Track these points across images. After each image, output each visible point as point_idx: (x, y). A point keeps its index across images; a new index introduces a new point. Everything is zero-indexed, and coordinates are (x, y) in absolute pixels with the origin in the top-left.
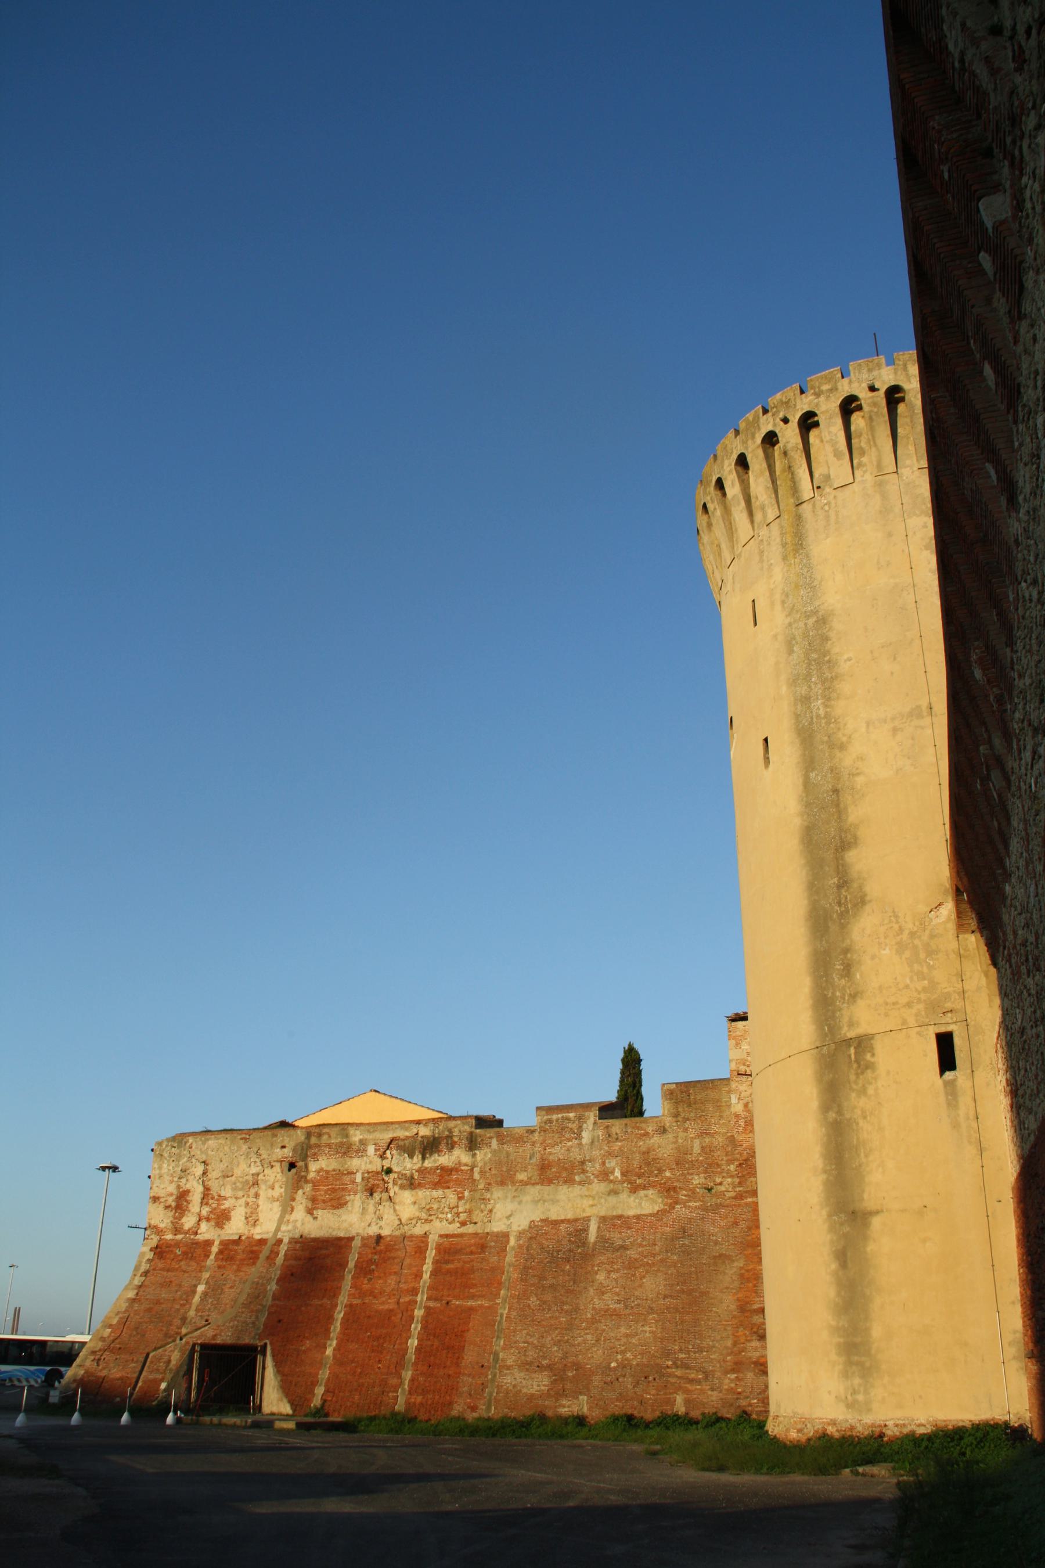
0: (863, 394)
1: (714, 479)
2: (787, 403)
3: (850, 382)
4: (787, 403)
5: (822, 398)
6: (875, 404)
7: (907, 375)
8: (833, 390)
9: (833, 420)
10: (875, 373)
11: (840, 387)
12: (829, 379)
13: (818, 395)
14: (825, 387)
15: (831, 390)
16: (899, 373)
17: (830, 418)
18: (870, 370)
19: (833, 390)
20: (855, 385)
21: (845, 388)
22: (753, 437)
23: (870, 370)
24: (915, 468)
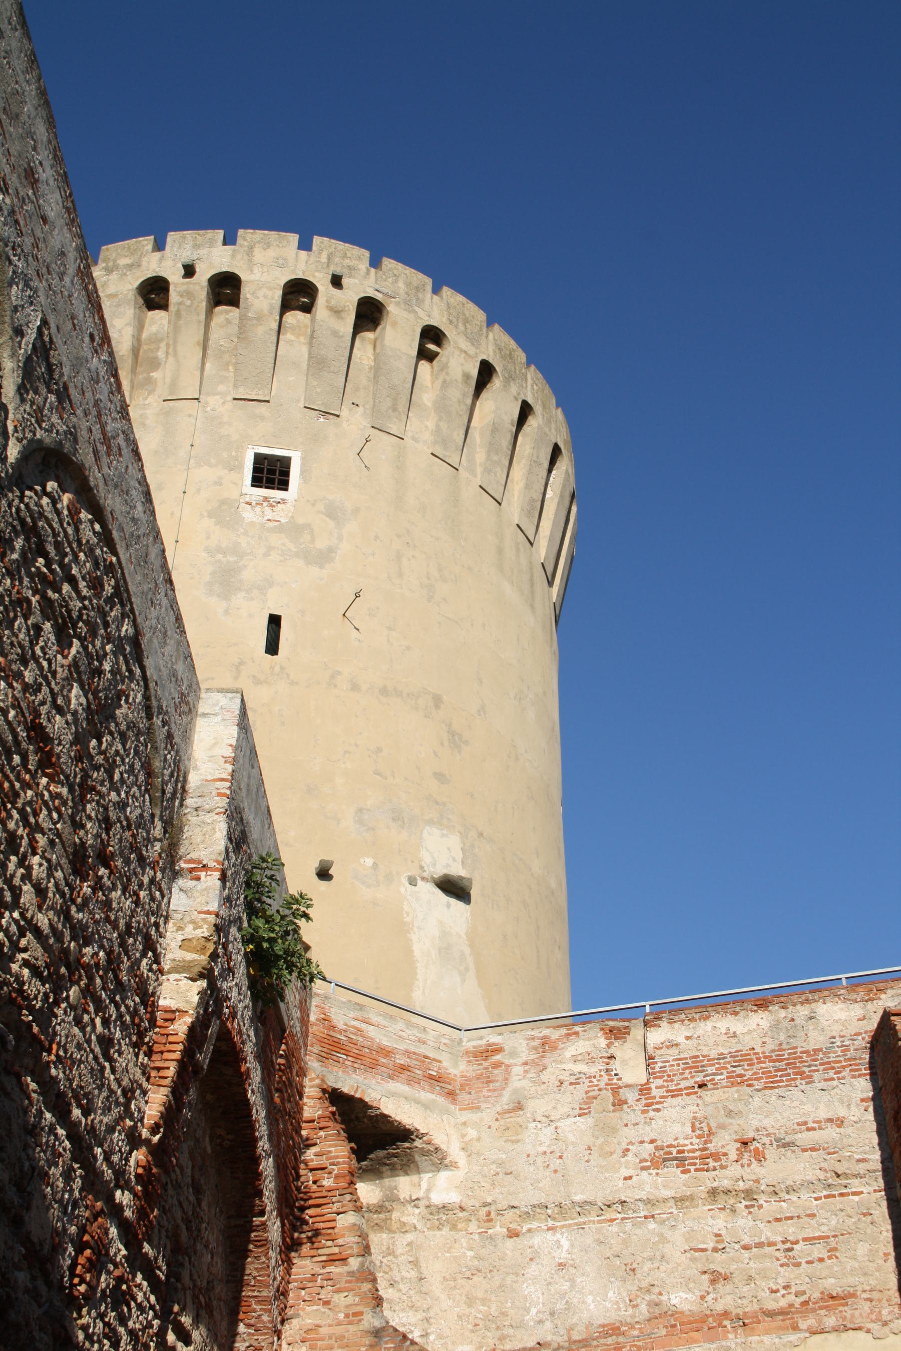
0: (174, 276)
3: (162, 259)
5: (114, 276)
6: (189, 294)
7: (250, 261)
9: (121, 309)
10: (203, 252)
11: (144, 263)
14: (123, 262)
15: (130, 267)
16: (239, 256)
17: (118, 305)
18: (196, 246)
20: (168, 263)
21: (154, 264)
23: (196, 246)
24: (230, 398)
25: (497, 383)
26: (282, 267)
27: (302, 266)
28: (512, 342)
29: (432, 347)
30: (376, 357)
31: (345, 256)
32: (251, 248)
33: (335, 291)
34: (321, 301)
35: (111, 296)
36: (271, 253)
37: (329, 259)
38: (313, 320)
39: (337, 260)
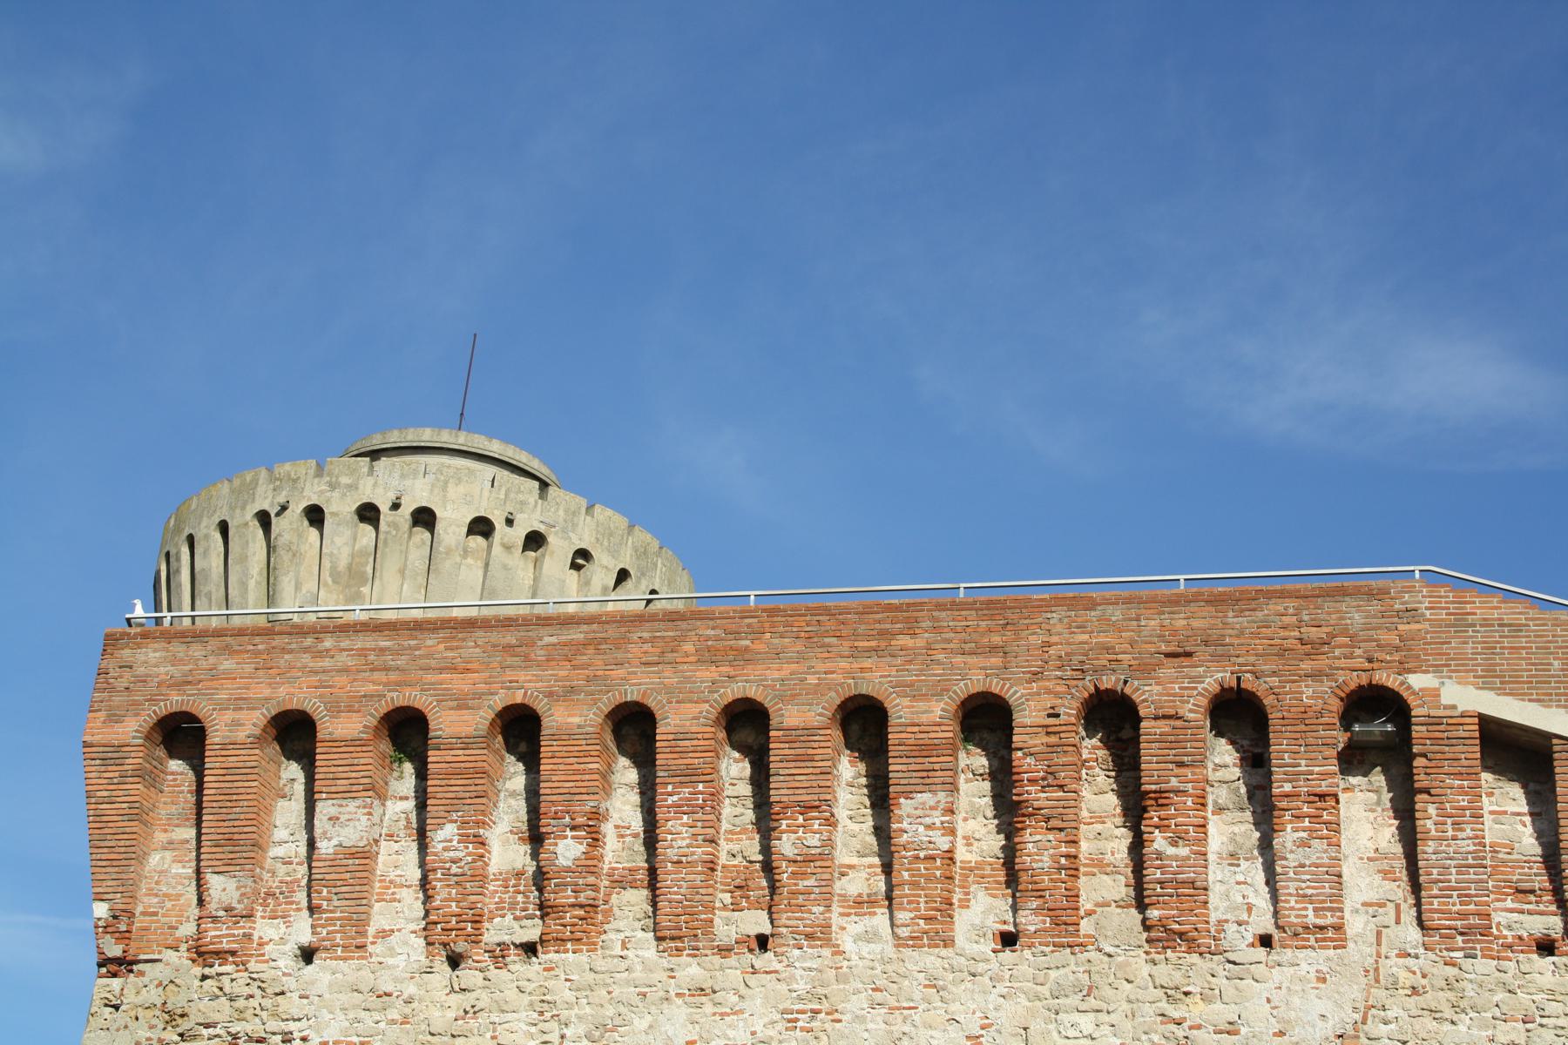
1: (186, 533)
2: (295, 481)
3: (375, 484)
4: (295, 481)
5: (336, 494)
6: (395, 525)
8: (353, 487)
10: (408, 483)
12: (353, 471)
13: (333, 486)
14: (345, 480)
15: (349, 487)
18: (403, 476)
19: (353, 487)
20: (380, 490)
22: (243, 508)
23: (403, 476)
25: (629, 584)
26: (469, 503)
27: (484, 503)
28: (649, 536)
29: (580, 561)
30: (535, 579)
31: (519, 491)
32: (446, 482)
33: (508, 529)
34: (497, 536)
35: (333, 514)
36: (461, 489)
37: (506, 495)
38: (490, 547)
39: (512, 495)
